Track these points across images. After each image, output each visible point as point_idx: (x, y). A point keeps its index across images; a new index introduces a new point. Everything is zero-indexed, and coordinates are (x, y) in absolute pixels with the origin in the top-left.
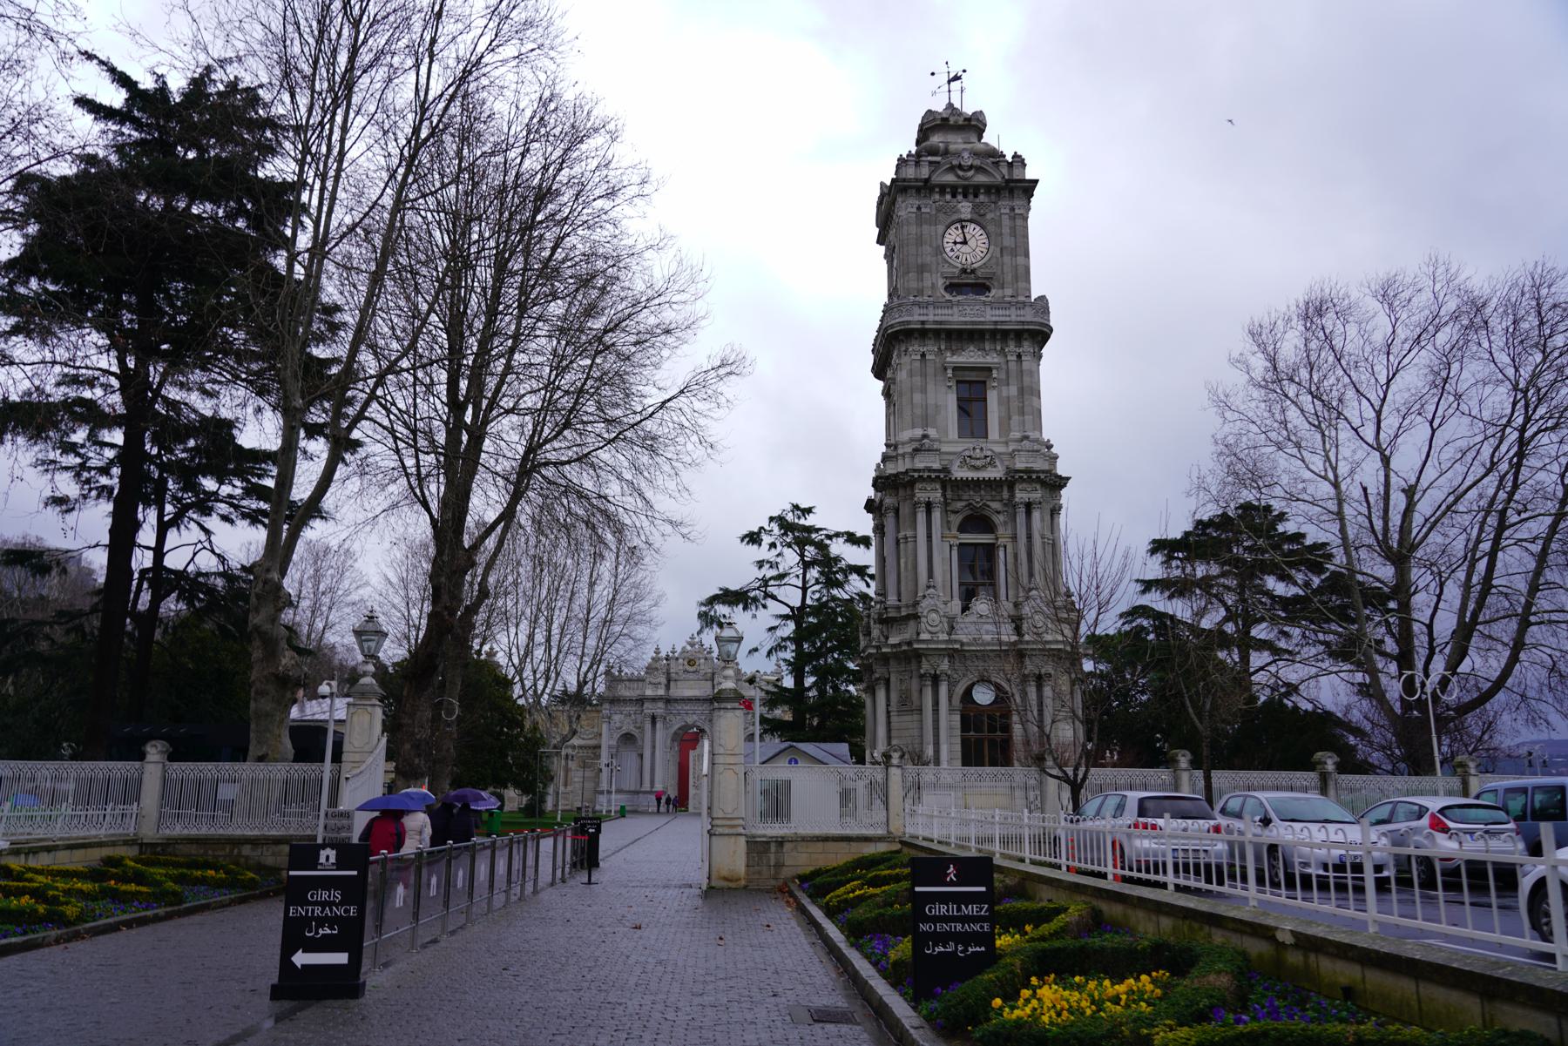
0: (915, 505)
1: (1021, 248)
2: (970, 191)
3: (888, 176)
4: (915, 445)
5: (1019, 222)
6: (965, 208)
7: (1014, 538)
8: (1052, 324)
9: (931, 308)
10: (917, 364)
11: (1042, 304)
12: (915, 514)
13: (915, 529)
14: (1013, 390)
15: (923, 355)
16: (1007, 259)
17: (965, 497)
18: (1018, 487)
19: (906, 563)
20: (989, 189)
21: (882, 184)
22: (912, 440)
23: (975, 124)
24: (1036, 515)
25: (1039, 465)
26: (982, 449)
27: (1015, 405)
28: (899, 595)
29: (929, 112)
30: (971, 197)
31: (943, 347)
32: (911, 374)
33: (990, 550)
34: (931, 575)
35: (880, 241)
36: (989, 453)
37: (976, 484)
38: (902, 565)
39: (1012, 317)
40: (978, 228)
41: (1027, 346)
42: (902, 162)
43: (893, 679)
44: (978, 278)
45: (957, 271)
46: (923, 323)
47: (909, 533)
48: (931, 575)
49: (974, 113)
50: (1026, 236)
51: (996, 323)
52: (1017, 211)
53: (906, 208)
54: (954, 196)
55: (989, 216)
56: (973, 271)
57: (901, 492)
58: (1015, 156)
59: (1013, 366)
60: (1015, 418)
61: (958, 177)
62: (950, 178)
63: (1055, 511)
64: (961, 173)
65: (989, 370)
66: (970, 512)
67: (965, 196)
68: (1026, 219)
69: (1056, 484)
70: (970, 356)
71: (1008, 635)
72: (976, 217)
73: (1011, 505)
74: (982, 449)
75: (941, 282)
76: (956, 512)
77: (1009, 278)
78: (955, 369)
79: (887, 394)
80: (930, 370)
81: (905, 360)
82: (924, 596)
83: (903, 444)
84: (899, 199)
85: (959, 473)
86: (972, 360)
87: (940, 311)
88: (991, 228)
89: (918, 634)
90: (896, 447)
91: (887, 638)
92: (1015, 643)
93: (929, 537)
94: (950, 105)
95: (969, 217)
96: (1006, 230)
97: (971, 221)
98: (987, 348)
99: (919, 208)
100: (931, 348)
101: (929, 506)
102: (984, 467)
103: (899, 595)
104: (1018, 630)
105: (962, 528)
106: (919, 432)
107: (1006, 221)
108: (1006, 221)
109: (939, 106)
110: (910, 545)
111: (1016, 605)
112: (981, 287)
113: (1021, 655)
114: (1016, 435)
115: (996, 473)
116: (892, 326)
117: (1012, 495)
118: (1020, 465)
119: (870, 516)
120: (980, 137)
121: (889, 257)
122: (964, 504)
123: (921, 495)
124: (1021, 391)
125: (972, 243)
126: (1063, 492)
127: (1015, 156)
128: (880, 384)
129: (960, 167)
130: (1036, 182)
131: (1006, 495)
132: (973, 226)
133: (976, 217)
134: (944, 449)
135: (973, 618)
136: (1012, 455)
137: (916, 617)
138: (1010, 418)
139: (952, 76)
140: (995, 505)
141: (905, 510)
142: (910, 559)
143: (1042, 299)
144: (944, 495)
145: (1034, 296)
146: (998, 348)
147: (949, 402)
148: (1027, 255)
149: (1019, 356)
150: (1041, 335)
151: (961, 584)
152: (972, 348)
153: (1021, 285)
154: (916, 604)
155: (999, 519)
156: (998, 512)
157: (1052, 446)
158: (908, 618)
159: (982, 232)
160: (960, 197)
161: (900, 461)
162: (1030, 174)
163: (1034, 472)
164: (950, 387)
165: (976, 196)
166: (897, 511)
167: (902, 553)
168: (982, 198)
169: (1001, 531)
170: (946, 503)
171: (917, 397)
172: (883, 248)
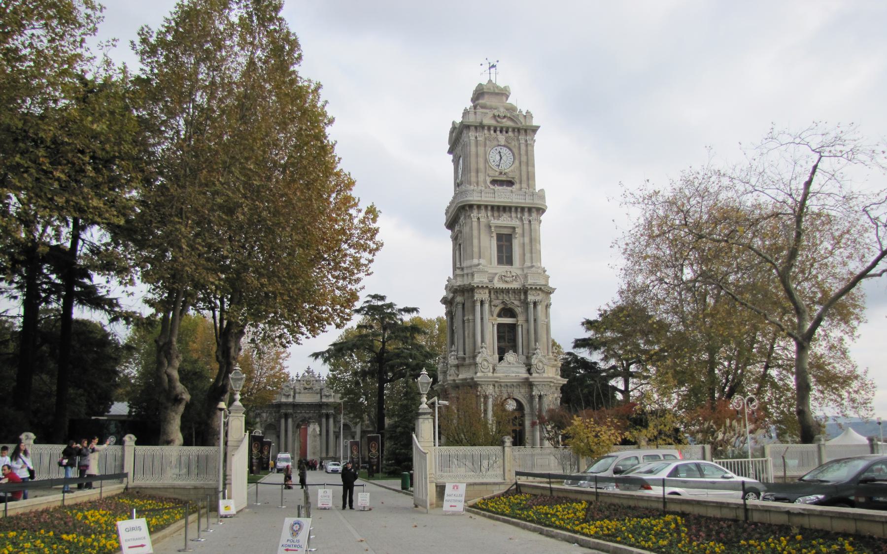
2: (504, 130)
3: (459, 120)
5: (529, 148)
6: (502, 138)
7: (527, 321)
8: (547, 204)
11: (541, 195)
13: (474, 315)
14: (527, 240)
19: (468, 334)
21: (454, 123)
23: (503, 93)
24: (539, 308)
27: (527, 248)
29: (480, 85)
33: (513, 327)
34: (483, 341)
36: (514, 274)
37: (508, 291)
38: (466, 335)
39: (527, 202)
40: (508, 150)
45: (497, 174)
46: (479, 201)
47: (471, 317)
48: (483, 341)
49: (505, 87)
51: (518, 203)
54: (495, 131)
57: (466, 294)
58: (527, 112)
59: (526, 227)
62: (493, 122)
63: (548, 306)
64: (499, 120)
65: (514, 228)
67: (501, 132)
68: (533, 147)
70: (505, 220)
71: (524, 374)
72: (506, 144)
73: (525, 303)
75: (489, 180)
77: (524, 178)
78: (496, 227)
79: (455, 239)
82: (479, 353)
83: (467, 267)
84: (465, 132)
85: (498, 284)
86: (505, 222)
89: (476, 373)
91: (458, 375)
92: (527, 379)
94: (490, 81)
97: (504, 146)
99: (476, 138)
100: (483, 213)
101: (482, 303)
104: (529, 371)
105: (499, 315)
109: (485, 82)
110: (471, 324)
112: (510, 183)
114: (528, 264)
115: (515, 285)
116: (461, 202)
117: (526, 298)
118: (530, 281)
119: (444, 306)
120: (507, 99)
122: (500, 301)
123: (478, 296)
124: (531, 240)
126: (551, 295)
127: (527, 112)
128: (449, 232)
130: (539, 127)
131: (522, 297)
133: (506, 144)
137: (476, 364)
139: (491, 64)
141: (468, 305)
142: (471, 331)
143: (542, 190)
144: (490, 296)
146: (519, 216)
149: (530, 221)
150: (541, 210)
154: (474, 357)
155: (518, 310)
157: (545, 271)
158: (470, 365)
160: (498, 132)
161: (465, 277)
165: (507, 132)
166: (463, 305)
167: (466, 328)
168: (510, 134)
170: (490, 302)
172: (451, 157)
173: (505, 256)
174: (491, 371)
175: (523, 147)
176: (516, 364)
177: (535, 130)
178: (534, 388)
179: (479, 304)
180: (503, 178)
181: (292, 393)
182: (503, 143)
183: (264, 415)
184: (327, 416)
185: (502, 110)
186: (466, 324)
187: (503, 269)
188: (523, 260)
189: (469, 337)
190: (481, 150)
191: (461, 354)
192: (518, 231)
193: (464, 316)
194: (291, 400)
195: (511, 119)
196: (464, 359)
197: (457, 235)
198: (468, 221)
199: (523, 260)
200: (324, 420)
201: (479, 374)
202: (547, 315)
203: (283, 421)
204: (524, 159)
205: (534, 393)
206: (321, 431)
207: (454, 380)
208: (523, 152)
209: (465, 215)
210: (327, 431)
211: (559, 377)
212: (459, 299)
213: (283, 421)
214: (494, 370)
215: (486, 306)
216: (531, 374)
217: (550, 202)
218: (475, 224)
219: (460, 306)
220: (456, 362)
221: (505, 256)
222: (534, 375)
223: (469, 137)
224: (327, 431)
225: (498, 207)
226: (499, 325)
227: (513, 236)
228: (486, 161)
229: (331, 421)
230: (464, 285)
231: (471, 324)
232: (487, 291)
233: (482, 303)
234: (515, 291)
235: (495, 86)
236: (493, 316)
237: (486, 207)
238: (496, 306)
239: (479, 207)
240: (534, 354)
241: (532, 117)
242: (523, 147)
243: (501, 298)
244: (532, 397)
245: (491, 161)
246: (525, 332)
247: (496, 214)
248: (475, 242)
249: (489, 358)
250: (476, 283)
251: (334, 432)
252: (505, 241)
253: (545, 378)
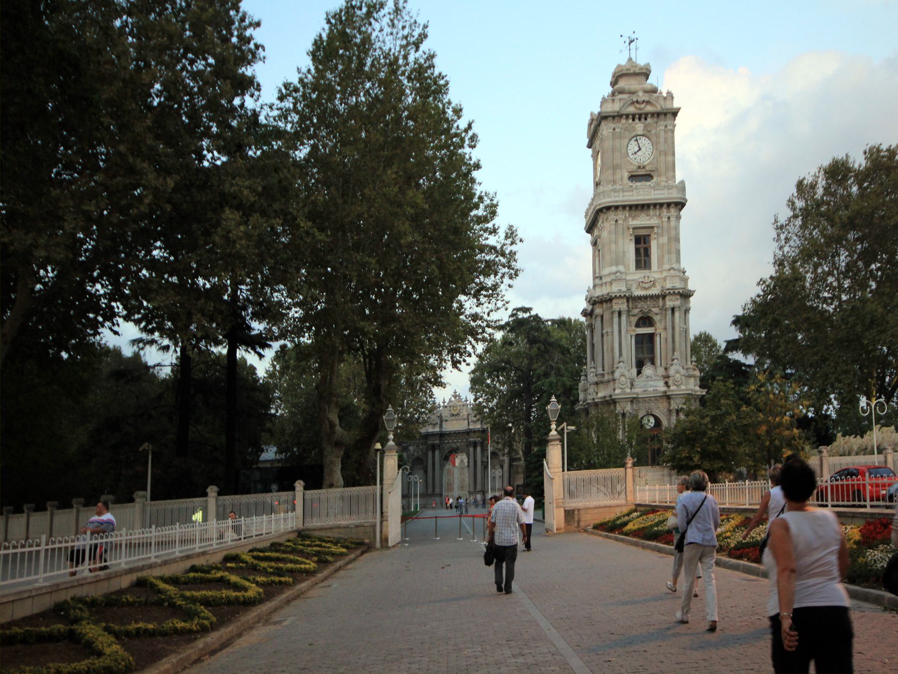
0: (613, 313)
1: (670, 151)
2: (642, 116)
3: (597, 110)
4: (612, 277)
5: (670, 134)
6: (639, 127)
7: (665, 329)
8: (687, 197)
9: (621, 193)
10: (613, 227)
11: (682, 187)
12: (612, 318)
13: (612, 327)
15: (616, 221)
16: (663, 157)
17: (639, 306)
18: (667, 298)
20: (653, 114)
22: (610, 274)
24: (677, 314)
25: (678, 284)
27: (666, 248)
28: (603, 367)
30: (643, 120)
31: (627, 216)
32: (609, 232)
33: (651, 337)
34: (621, 355)
35: (590, 146)
37: (645, 298)
40: (647, 139)
41: (673, 211)
42: (604, 101)
44: (647, 171)
48: (621, 355)
50: (673, 143)
52: (669, 128)
53: (606, 129)
54: (633, 120)
55: (653, 132)
56: (644, 167)
58: (669, 93)
60: (666, 256)
61: (636, 108)
62: (631, 110)
63: (687, 311)
64: (638, 106)
66: (642, 315)
67: (640, 119)
68: (673, 132)
69: (686, 295)
71: (661, 387)
72: (646, 133)
73: (664, 309)
75: (626, 175)
76: (635, 316)
78: (634, 228)
80: (620, 230)
81: (606, 224)
82: (618, 368)
83: (605, 276)
86: (643, 222)
87: (625, 194)
88: (654, 139)
89: (614, 390)
90: (601, 278)
92: (665, 392)
93: (620, 331)
95: (642, 133)
96: (662, 140)
97: (643, 135)
98: (651, 214)
101: (620, 313)
102: (649, 288)
103: (603, 367)
105: (637, 325)
106: (614, 269)
107: (662, 133)
108: (662, 133)
110: (610, 337)
111: (666, 369)
112: (648, 177)
113: (669, 398)
115: (655, 291)
116: (600, 205)
117: (664, 304)
121: (595, 157)
122: (639, 310)
124: (669, 239)
125: (643, 149)
127: (669, 93)
129: (637, 102)
130: (679, 109)
132: (644, 138)
133: (646, 133)
134: (629, 277)
135: (644, 378)
136: (665, 279)
138: (663, 256)
140: (655, 310)
143: (682, 183)
144: (628, 306)
145: (677, 181)
147: (631, 248)
148: (674, 155)
151: (636, 358)
153: (671, 174)
155: (656, 318)
156: (657, 314)
157: (684, 273)
158: (609, 381)
159: (649, 141)
160: (637, 121)
161: (604, 287)
162: (676, 105)
164: (631, 240)
165: (646, 119)
168: (649, 120)
169: (658, 325)
170: (629, 311)
171: (613, 246)
173: (643, 258)
174: (629, 386)
176: (654, 377)
177: (675, 113)
178: (672, 402)
179: (616, 315)
180: (642, 172)
181: (439, 422)
183: (411, 448)
184: (475, 445)
185: (641, 94)
187: (640, 275)
194: (437, 429)
196: (603, 375)
200: (471, 449)
201: (617, 391)
202: (686, 321)
203: (430, 454)
205: (671, 408)
206: (468, 462)
207: (593, 399)
210: (475, 462)
211: (698, 388)
212: (598, 311)
213: (430, 454)
214: (632, 385)
215: (624, 318)
216: (668, 387)
217: (690, 196)
220: (596, 379)
221: (643, 258)
222: (672, 388)
224: (475, 462)
226: (637, 335)
229: (479, 449)
230: (603, 296)
231: (610, 337)
232: (625, 300)
233: (620, 313)
234: (652, 297)
235: (635, 65)
236: (631, 326)
237: (624, 207)
239: (617, 207)
240: (672, 365)
241: (673, 98)
243: (639, 306)
244: (670, 411)
249: (627, 374)
250: (615, 293)
251: (482, 462)
252: (642, 243)
253: (683, 390)
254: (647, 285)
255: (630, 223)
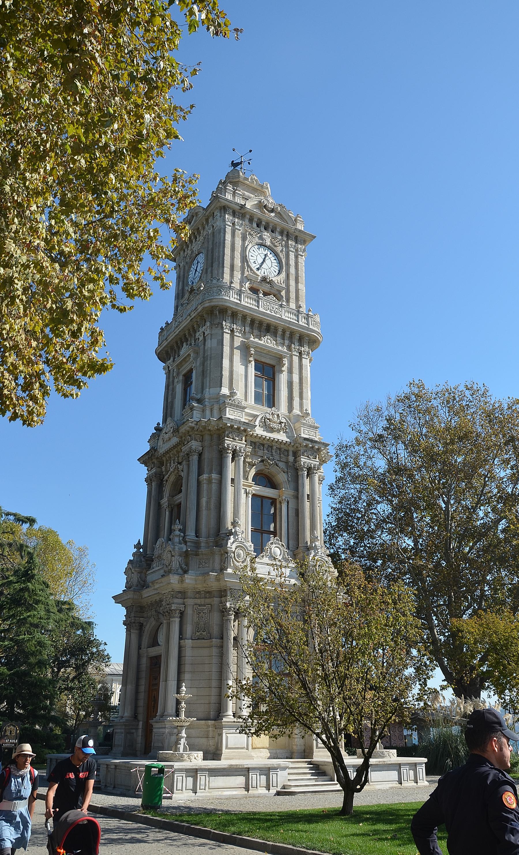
6: (267, 236)
14: (296, 378)
19: (208, 503)
26: (278, 415)
36: (284, 420)
43: (189, 611)
47: (214, 476)
54: (258, 226)
59: (296, 359)
67: (265, 229)
74: (278, 415)
85: (259, 431)
97: (269, 248)
101: (235, 454)
118: (303, 435)
123: (228, 442)
129: (265, 206)
131: (291, 458)
152: (269, 337)
160: (262, 229)
163: (316, 442)
166: (200, 455)
175: (292, 256)
182: (268, 243)
186: (205, 487)
188: (290, 408)
189: (208, 509)
190: (238, 242)
191: (191, 533)
192: (286, 361)
193: (200, 474)
195: (279, 215)
197: (189, 355)
198: (215, 331)
199: (290, 408)
204: (292, 270)
208: (292, 262)
209: (211, 324)
218: (227, 337)
219: (195, 458)
223: (224, 220)
225: (261, 323)
227: (277, 368)
228: (244, 259)
236: (247, 479)
238: (251, 465)
242: (292, 256)
245: (252, 261)
246: (292, 513)
247: (256, 332)
248: (226, 363)
254: (273, 425)
255: (252, 339)
